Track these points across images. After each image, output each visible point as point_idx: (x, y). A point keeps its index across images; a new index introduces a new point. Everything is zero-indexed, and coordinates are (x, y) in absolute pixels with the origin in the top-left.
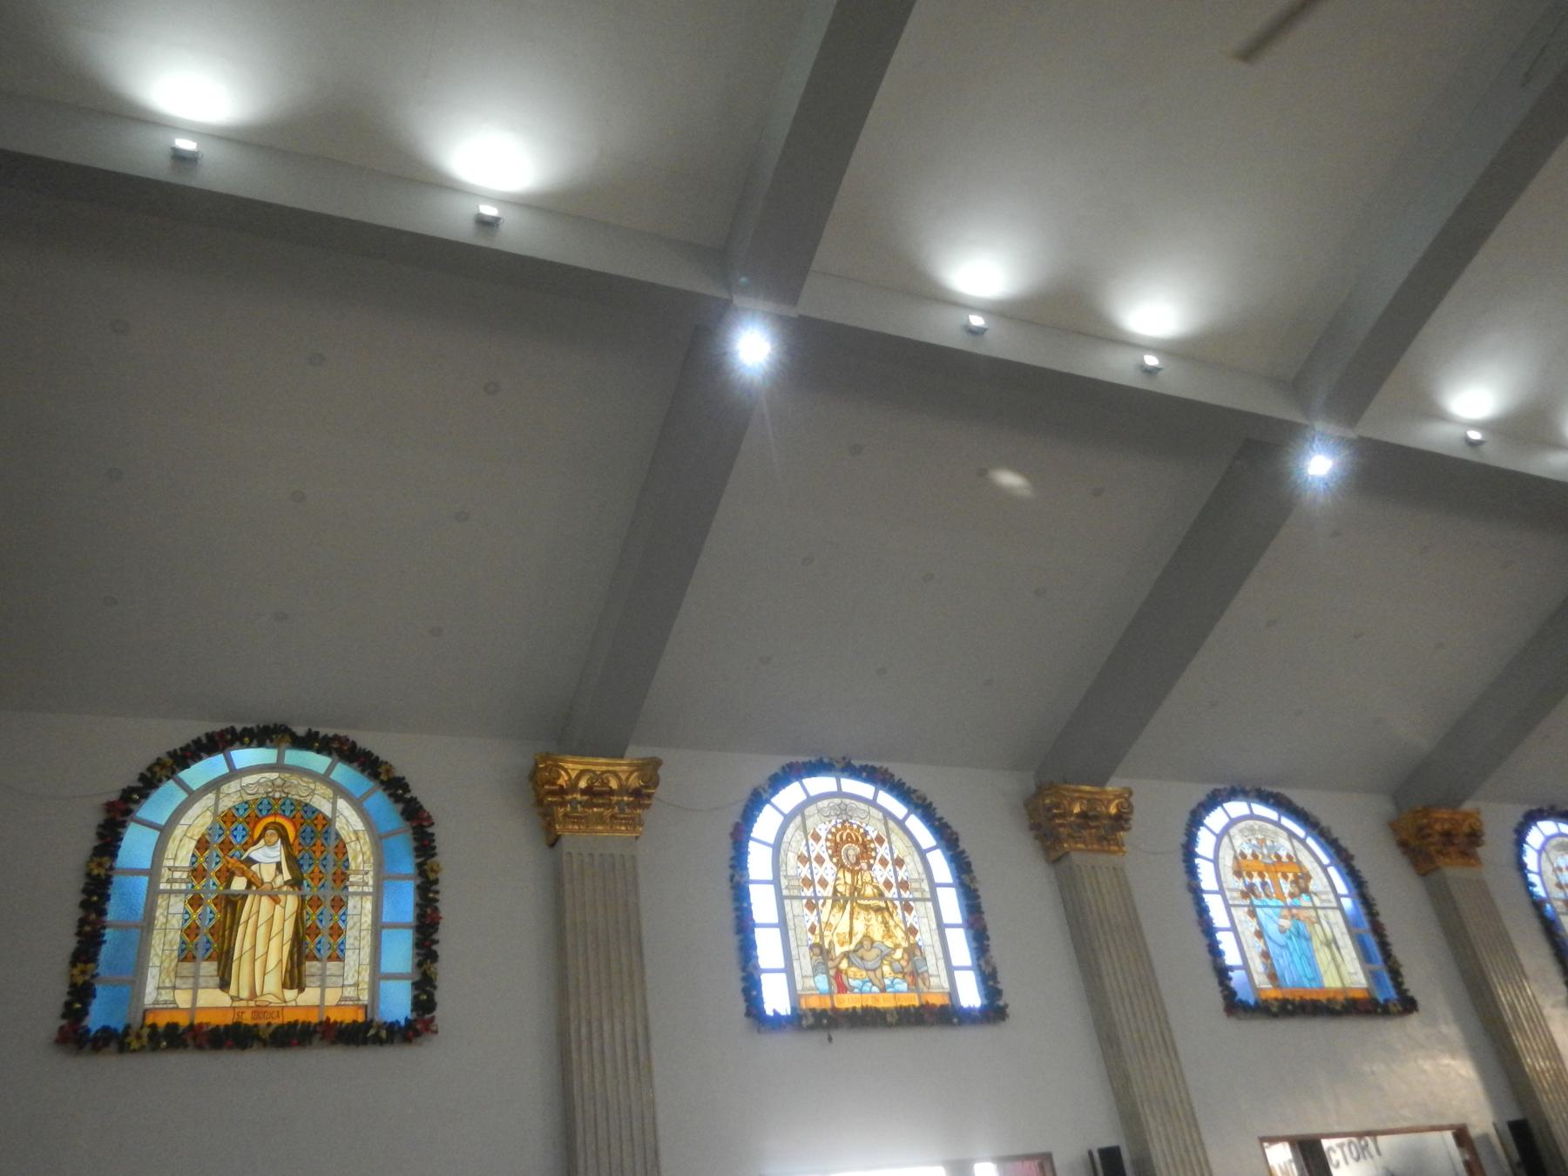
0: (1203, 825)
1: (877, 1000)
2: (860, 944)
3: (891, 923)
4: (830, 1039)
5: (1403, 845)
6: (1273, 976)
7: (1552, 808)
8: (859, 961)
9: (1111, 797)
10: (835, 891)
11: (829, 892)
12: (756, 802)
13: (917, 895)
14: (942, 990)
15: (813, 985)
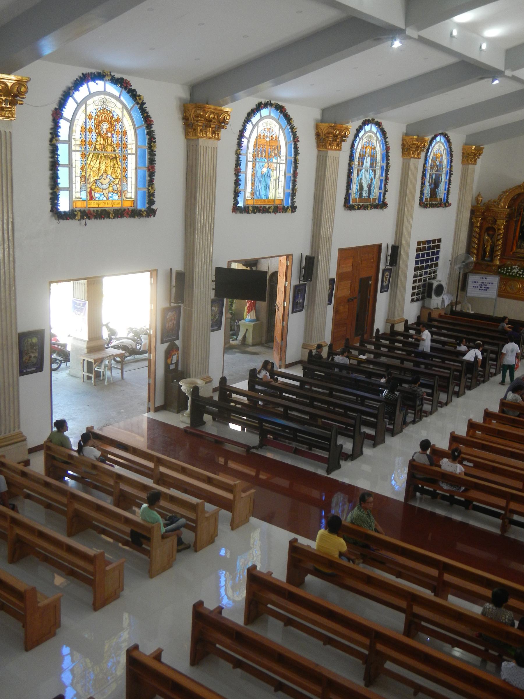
0: (250, 121)
1: (104, 204)
2: (102, 175)
3: (117, 166)
4: (86, 225)
5: (318, 135)
6: (253, 194)
7: (373, 120)
8: (100, 184)
9: (223, 112)
10: (95, 148)
11: (93, 147)
12: (67, 95)
13: (129, 151)
14: (131, 199)
15: (80, 196)
